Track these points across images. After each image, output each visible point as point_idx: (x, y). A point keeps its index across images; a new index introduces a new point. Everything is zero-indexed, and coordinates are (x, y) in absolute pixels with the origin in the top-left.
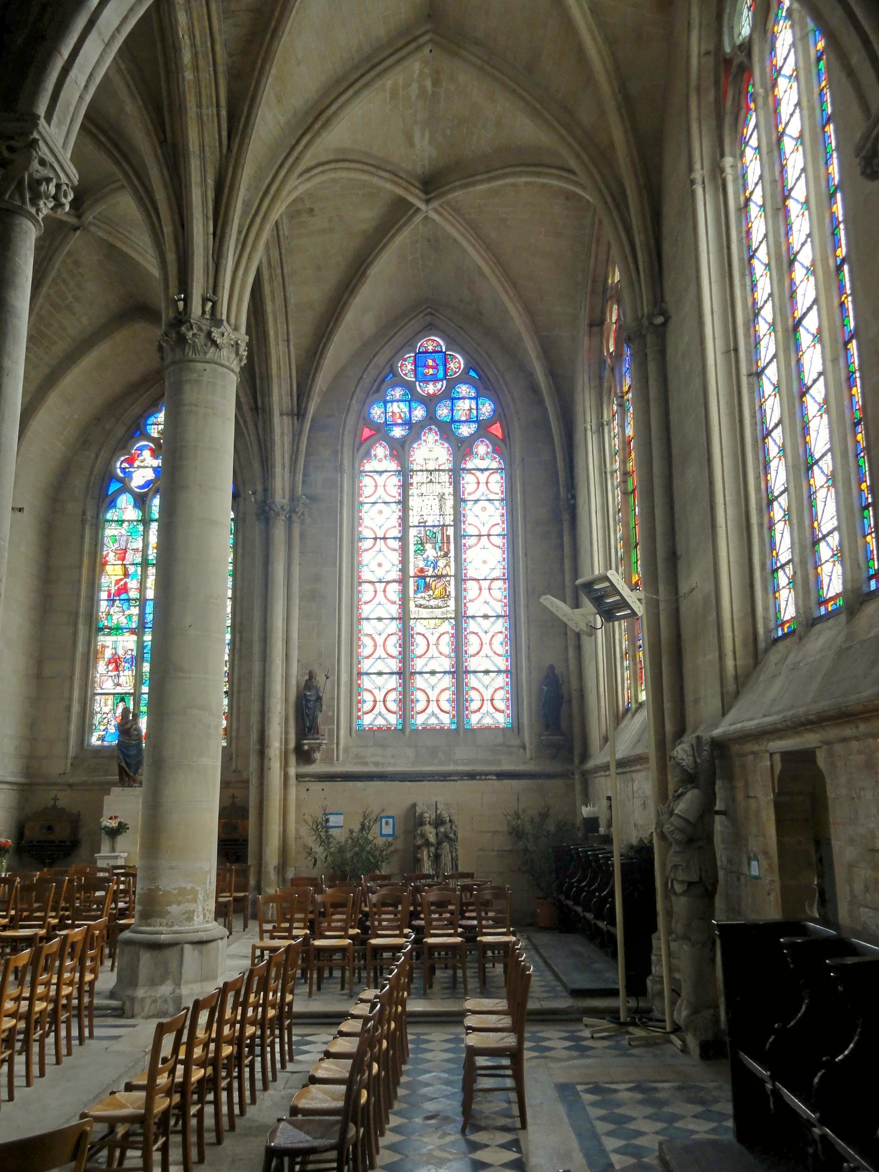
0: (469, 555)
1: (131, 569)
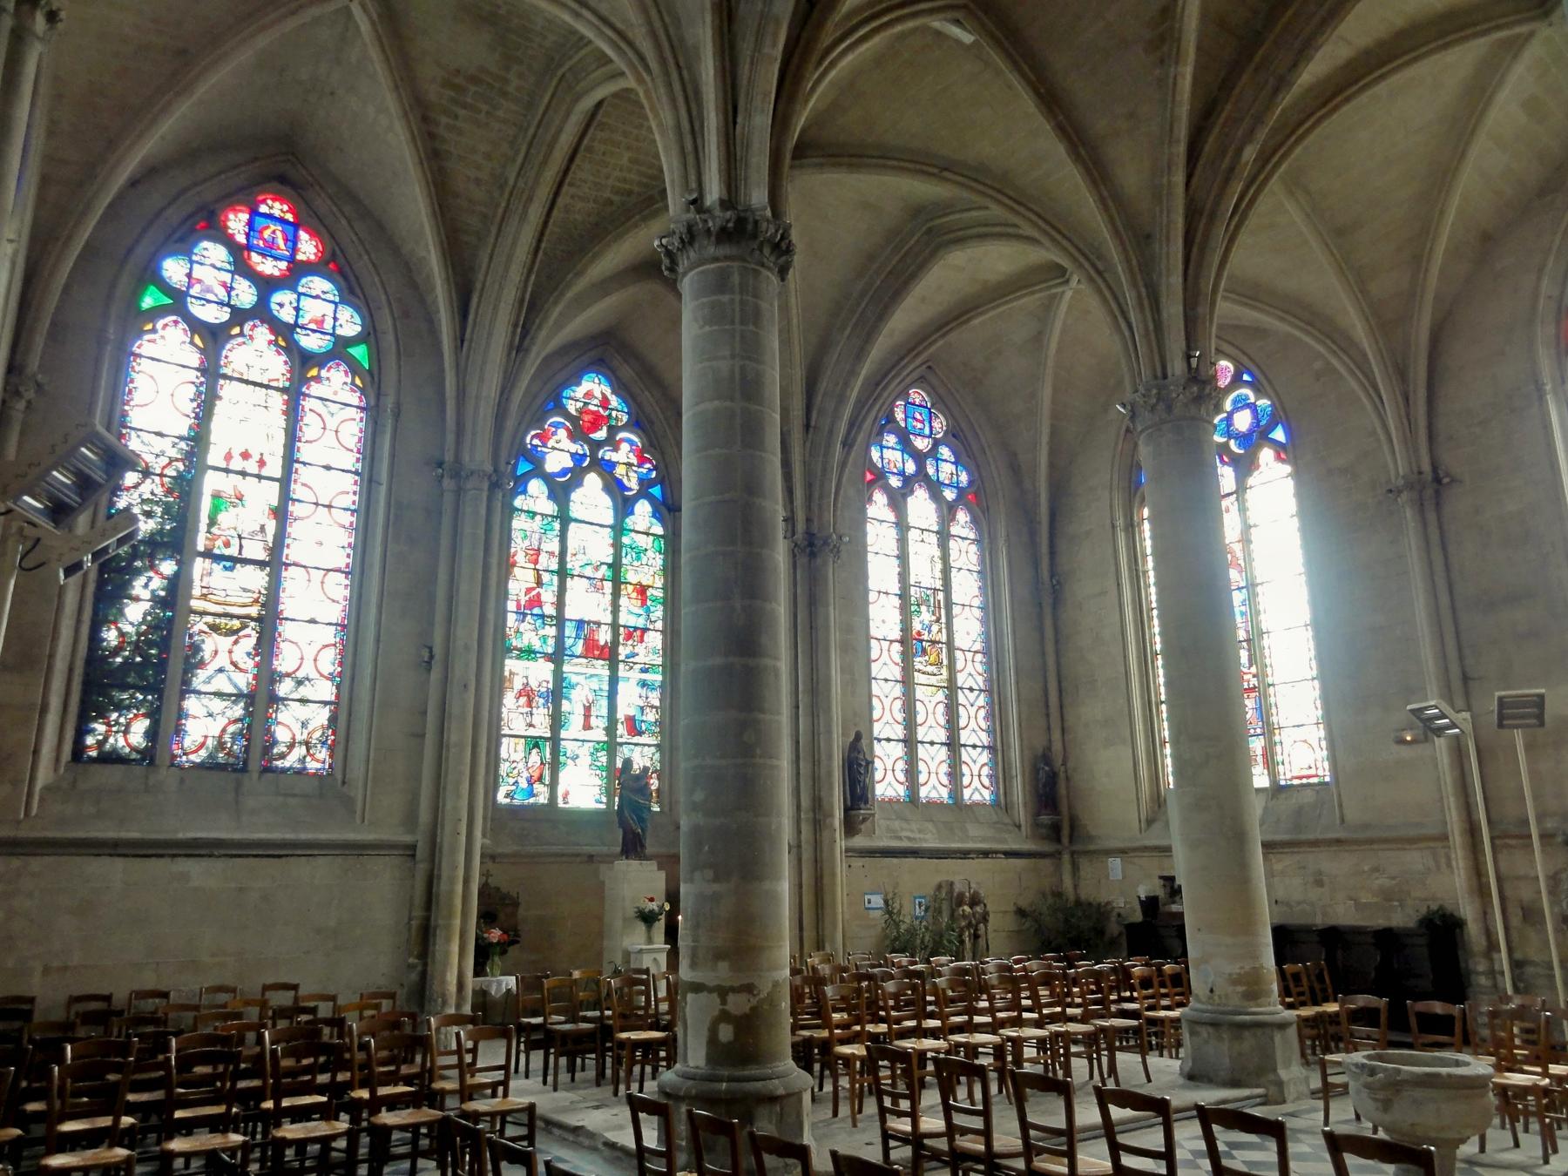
0: (956, 623)
1: (546, 577)
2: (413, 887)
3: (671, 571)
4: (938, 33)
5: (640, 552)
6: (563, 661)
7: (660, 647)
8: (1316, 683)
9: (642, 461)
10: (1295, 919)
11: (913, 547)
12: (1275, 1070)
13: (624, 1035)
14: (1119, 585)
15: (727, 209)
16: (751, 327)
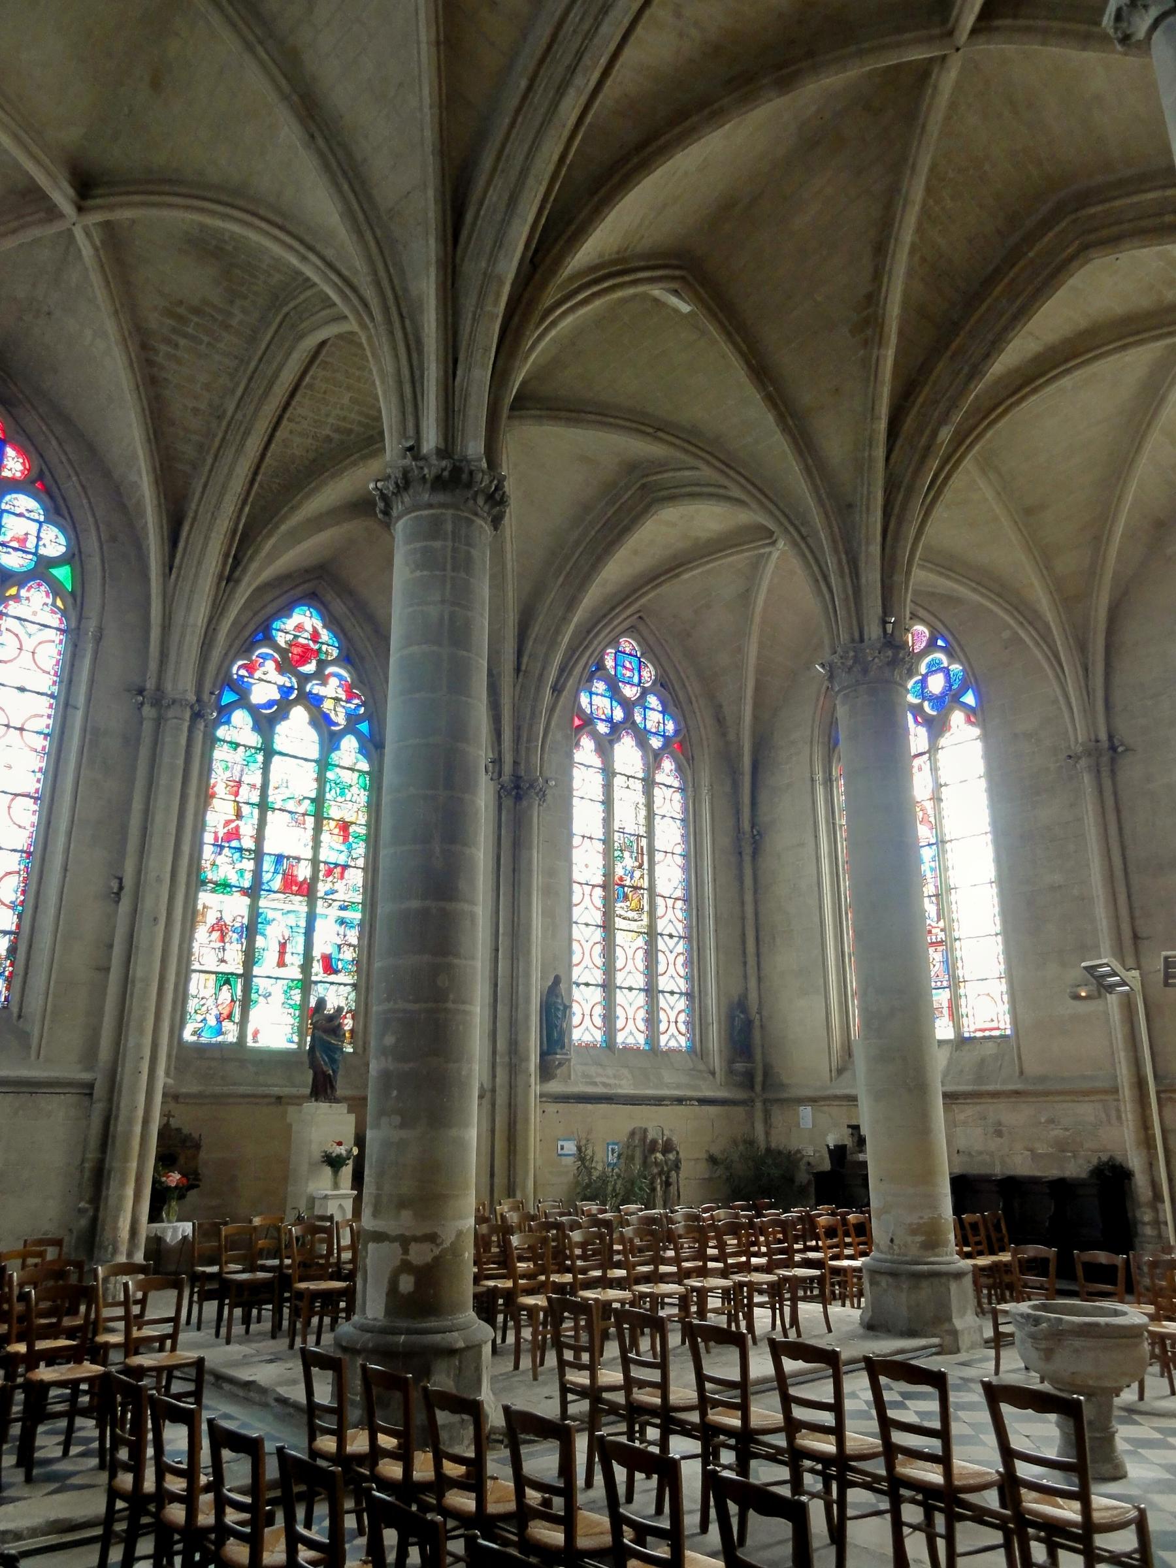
1: (246, 810)
2: (88, 1126)
3: (374, 808)
4: (656, 301)
5: (344, 788)
6: (259, 897)
7: (360, 884)
8: (999, 938)
9: (350, 697)
10: (975, 1169)
11: (618, 793)
12: (949, 1319)
13: (303, 1285)
14: (816, 837)
15: (443, 458)
16: (463, 575)
